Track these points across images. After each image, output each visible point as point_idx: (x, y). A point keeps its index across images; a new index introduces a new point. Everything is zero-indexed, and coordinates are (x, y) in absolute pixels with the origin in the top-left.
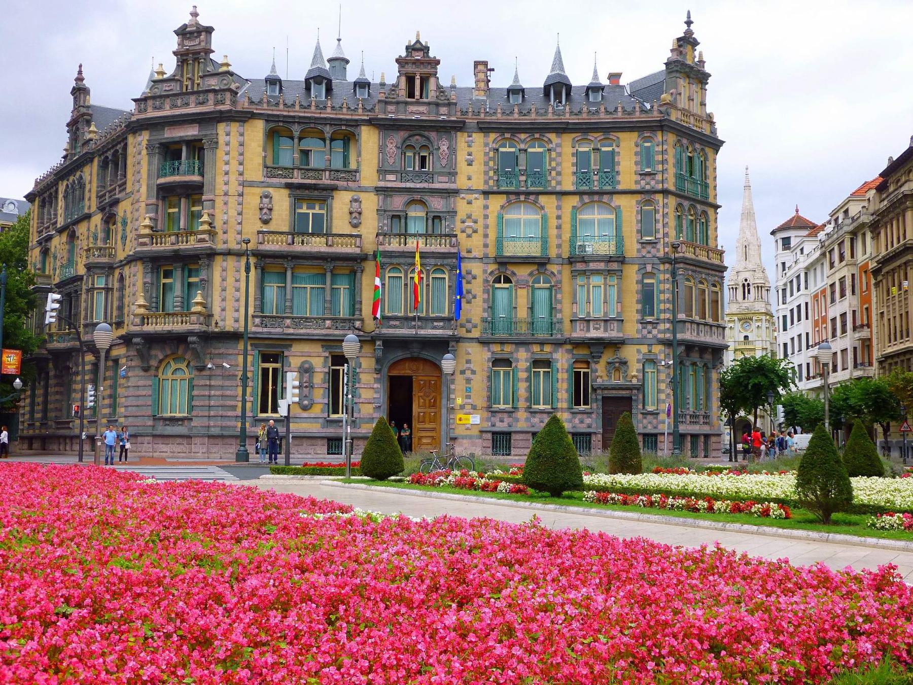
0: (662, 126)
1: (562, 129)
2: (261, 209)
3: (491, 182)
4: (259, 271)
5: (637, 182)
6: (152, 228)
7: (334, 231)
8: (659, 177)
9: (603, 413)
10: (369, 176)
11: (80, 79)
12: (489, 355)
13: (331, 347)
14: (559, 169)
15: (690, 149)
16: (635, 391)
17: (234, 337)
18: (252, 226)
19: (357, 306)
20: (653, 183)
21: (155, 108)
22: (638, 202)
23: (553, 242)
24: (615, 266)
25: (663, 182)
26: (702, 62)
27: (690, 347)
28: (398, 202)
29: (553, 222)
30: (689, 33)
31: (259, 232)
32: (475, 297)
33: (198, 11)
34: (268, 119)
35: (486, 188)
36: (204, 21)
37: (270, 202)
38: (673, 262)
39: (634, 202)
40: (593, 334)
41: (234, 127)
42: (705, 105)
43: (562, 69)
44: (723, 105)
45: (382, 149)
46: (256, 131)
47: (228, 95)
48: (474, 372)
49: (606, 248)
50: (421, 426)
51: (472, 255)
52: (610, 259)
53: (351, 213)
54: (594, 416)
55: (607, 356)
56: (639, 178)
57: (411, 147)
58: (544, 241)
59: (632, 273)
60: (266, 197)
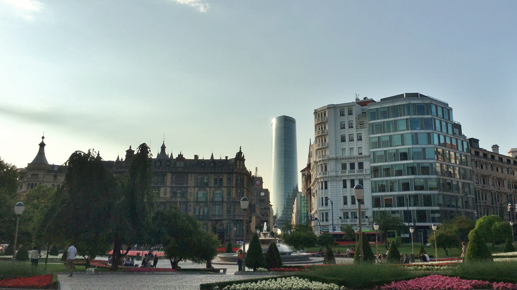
10: (168, 184)
26: (244, 156)
29: (209, 194)
30: (240, 151)
38: (234, 202)
40: (216, 218)
45: (172, 178)
49: (220, 199)
52: (220, 202)
55: (220, 222)
59: (225, 205)
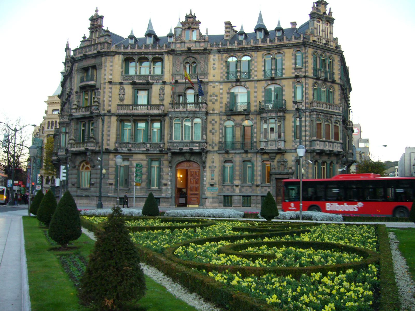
0: (305, 44)
1: (257, 49)
2: (119, 95)
3: (224, 77)
4: (119, 122)
5: (293, 73)
6: (77, 105)
7: (139, 103)
8: (303, 70)
9: (277, 186)
11: (68, 45)
12: (241, 159)
13: (150, 156)
14: (256, 69)
15: (323, 55)
16: (291, 176)
17: (108, 152)
18: (116, 102)
19: (162, 137)
20: (300, 73)
21: (79, 53)
22: (294, 83)
23: (253, 104)
24: (281, 114)
25: (305, 72)
26: (330, 13)
27: (321, 153)
28: (180, 89)
31: (118, 105)
32: (216, 132)
33: (98, 9)
34: (124, 54)
35: (222, 80)
36: (100, 14)
37: (124, 92)
39: (291, 83)
41: (109, 58)
42: (332, 34)
43: (262, 21)
44: (341, 32)
46: (118, 60)
47: (106, 45)
48: (215, 167)
50: (192, 192)
51: (215, 112)
53: (160, 95)
54: (271, 188)
56: (294, 71)
57: (187, 63)
58: (249, 104)
60: (122, 89)
